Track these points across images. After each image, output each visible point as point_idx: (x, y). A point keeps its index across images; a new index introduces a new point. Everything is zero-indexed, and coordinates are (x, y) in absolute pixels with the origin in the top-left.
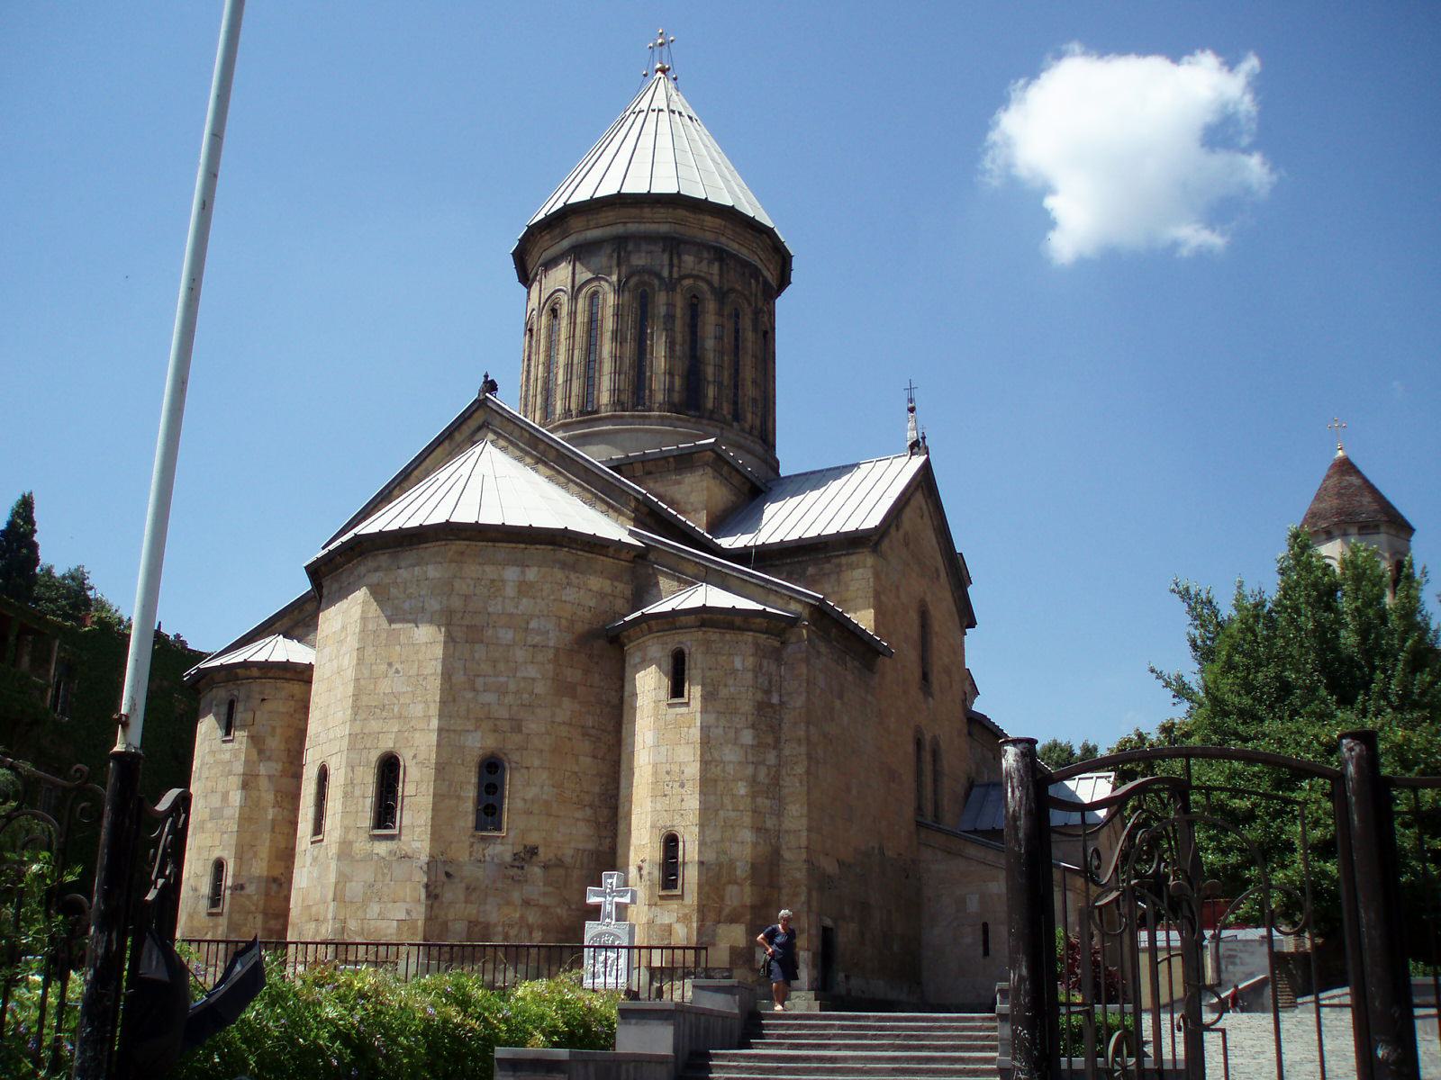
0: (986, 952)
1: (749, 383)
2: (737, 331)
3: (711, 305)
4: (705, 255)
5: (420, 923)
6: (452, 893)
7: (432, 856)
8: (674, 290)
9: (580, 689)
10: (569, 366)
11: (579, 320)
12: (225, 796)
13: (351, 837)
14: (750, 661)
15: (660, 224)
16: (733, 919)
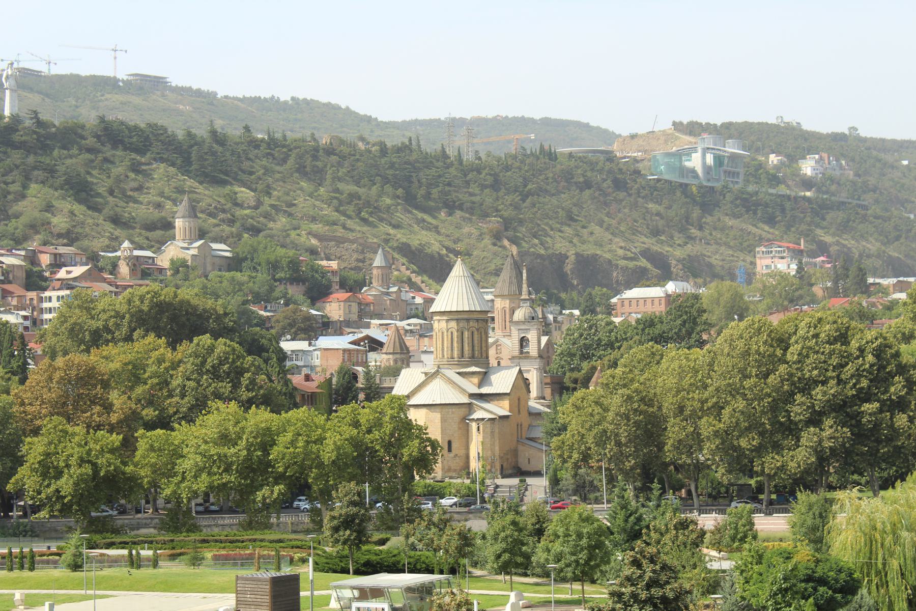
3: (476, 333)
6: (445, 462)
10: (447, 347)
15: (465, 316)
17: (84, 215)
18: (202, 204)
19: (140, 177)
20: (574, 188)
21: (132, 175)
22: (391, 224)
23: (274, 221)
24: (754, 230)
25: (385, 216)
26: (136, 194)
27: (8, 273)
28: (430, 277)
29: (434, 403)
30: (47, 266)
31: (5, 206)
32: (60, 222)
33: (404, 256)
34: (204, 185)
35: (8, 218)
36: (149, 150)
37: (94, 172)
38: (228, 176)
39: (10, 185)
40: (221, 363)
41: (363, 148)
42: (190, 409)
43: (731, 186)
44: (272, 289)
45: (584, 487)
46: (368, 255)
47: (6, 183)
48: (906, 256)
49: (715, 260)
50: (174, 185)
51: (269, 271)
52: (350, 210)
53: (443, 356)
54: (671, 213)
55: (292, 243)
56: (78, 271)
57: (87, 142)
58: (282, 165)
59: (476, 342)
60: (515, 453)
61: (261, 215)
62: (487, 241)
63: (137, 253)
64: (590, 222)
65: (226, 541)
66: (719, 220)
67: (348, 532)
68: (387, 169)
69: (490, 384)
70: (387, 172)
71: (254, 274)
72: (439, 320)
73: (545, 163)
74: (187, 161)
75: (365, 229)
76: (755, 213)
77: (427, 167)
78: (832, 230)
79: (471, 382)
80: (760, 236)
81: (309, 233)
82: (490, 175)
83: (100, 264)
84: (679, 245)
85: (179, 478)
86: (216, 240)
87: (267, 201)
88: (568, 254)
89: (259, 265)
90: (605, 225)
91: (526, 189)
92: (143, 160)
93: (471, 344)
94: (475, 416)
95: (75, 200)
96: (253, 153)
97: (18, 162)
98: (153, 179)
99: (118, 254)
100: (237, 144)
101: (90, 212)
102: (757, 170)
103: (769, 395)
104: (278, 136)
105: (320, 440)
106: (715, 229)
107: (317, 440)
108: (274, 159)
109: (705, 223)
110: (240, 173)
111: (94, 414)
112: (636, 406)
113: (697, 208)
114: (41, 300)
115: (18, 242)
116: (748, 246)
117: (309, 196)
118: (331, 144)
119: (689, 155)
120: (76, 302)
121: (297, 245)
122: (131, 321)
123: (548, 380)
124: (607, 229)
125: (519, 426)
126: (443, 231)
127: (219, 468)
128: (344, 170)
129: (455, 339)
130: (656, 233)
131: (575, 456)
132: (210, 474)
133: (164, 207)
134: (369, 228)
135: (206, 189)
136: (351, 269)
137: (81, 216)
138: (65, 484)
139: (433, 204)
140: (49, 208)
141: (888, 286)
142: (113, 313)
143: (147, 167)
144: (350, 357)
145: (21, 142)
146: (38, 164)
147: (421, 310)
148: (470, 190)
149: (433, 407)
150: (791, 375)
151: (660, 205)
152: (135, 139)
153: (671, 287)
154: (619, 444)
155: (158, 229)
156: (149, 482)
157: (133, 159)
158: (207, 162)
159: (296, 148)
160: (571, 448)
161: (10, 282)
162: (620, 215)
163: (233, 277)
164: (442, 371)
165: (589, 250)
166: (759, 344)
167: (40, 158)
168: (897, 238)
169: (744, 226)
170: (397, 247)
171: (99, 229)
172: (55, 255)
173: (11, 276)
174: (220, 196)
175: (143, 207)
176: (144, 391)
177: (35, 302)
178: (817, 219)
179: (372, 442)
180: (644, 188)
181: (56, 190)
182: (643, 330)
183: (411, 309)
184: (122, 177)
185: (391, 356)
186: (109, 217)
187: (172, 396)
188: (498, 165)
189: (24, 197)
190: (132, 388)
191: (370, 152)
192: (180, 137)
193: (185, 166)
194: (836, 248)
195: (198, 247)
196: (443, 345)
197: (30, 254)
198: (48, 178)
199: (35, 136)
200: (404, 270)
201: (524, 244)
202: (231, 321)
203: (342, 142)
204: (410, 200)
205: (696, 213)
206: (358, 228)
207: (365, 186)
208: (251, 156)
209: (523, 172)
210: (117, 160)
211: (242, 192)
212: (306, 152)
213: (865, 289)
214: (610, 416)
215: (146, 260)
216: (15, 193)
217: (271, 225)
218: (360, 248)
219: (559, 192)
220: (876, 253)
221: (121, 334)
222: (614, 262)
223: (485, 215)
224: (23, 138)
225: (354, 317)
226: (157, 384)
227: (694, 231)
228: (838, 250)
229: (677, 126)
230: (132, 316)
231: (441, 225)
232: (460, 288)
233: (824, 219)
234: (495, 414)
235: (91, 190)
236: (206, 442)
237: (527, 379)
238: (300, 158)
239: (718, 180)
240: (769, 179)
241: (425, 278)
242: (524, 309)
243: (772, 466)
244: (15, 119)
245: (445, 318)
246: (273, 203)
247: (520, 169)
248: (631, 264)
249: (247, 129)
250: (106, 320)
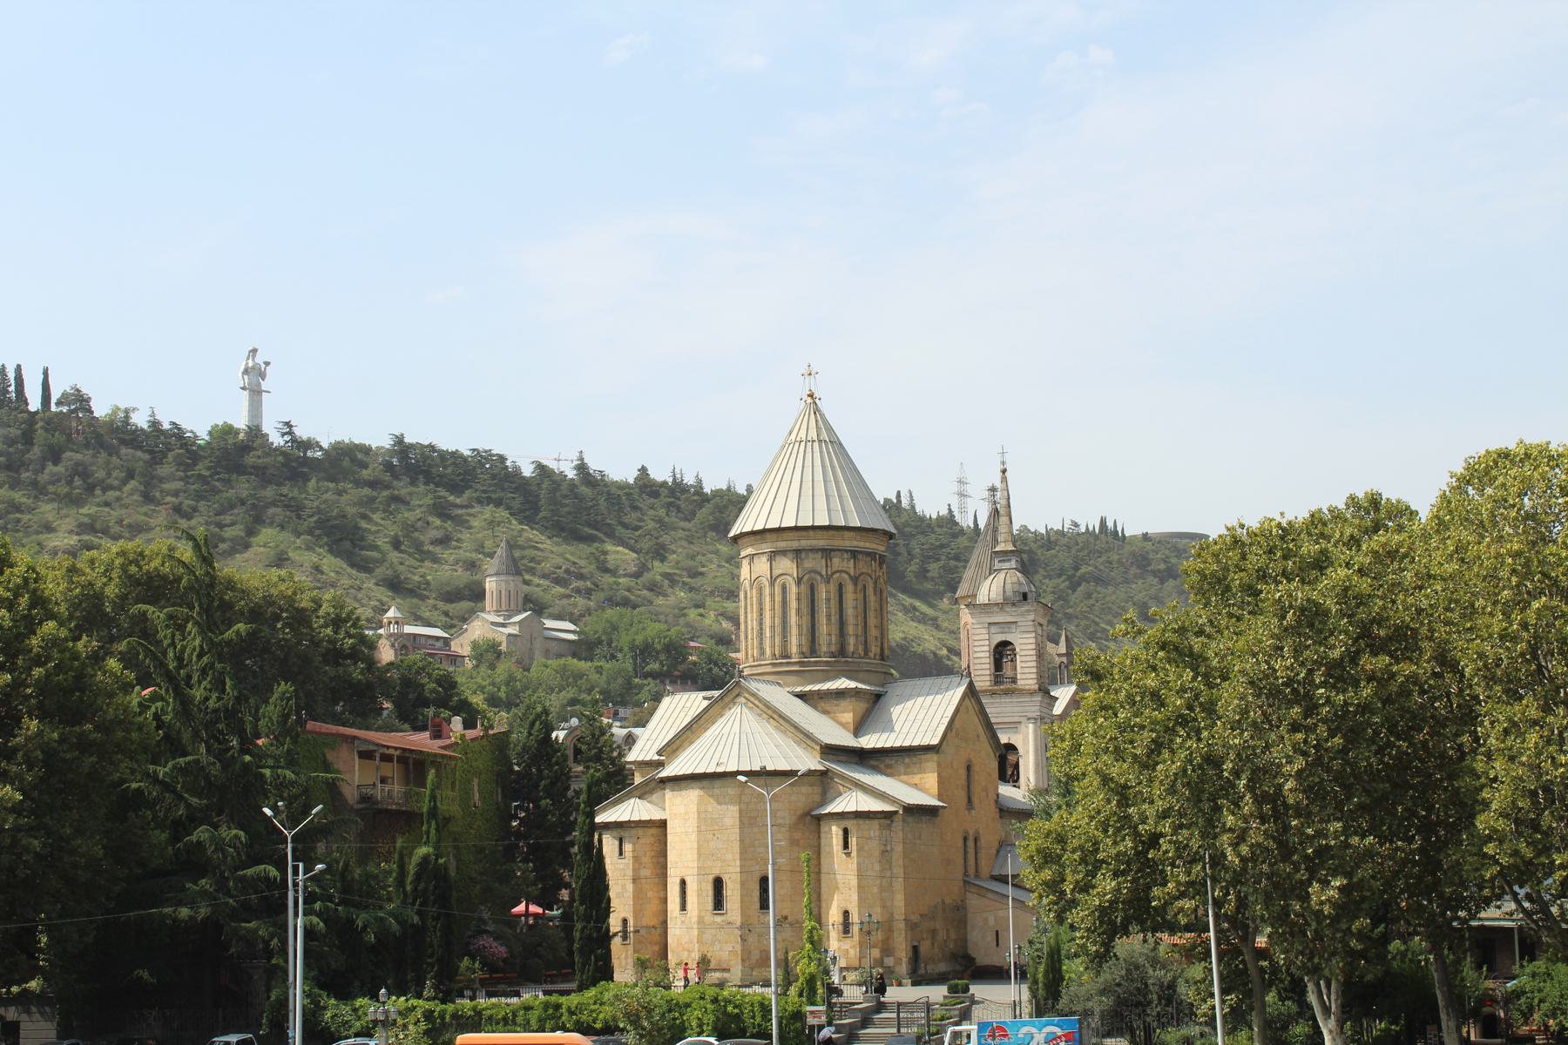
0: (998, 945)
1: (873, 629)
2: (865, 596)
3: (849, 588)
4: (846, 556)
5: (739, 952)
6: (751, 939)
7: (742, 924)
8: (828, 582)
9: (801, 842)
10: (773, 627)
11: (776, 599)
12: (624, 886)
13: (703, 914)
14: (877, 833)
15: (820, 542)
16: (875, 947)
17: (337, 572)
21: (438, 522)
23: (665, 595)
26: (438, 549)
29: (720, 769)
34: (555, 539)
36: (471, 487)
37: (376, 517)
38: (597, 530)
39: (226, 529)
45: (1143, 1005)
51: (635, 660)
58: (689, 521)
59: (850, 612)
60: (958, 915)
72: (752, 557)
73: (1107, 542)
74: (536, 509)
77: (923, 533)
89: (621, 650)
91: (1078, 574)
92: (458, 501)
93: (835, 618)
94: (836, 806)
95: (331, 551)
96: (645, 502)
97: (244, 494)
98: (470, 528)
101: (349, 570)
108: (679, 511)
110: (619, 527)
117: (727, 562)
125: (971, 842)
126: (945, 625)
129: (793, 604)
131: (1106, 884)
135: (558, 544)
137: (332, 574)
143: (464, 511)
146: (278, 497)
149: (718, 783)
157: (440, 497)
158: (567, 509)
160: (1091, 861)
163: (565, 665)
175: (447, 567)
186: (383, 580)
189: (247, 546)
195: (520, 623)
196: (761, 624)
202: (350, 636)
209: (1073, 552)
211: (618, 552)
215: (430, 642)
216: (232, 540)
217: (660, 601)
219: (1127, 581)
231: (942, 617)
232: (808, 470)
237: (1011, 748)
238: (721, 512)
242: (1002, 575)
245: (766, 547)
246: (668, 571)
247: (1069, 548)
249: (643, 470)
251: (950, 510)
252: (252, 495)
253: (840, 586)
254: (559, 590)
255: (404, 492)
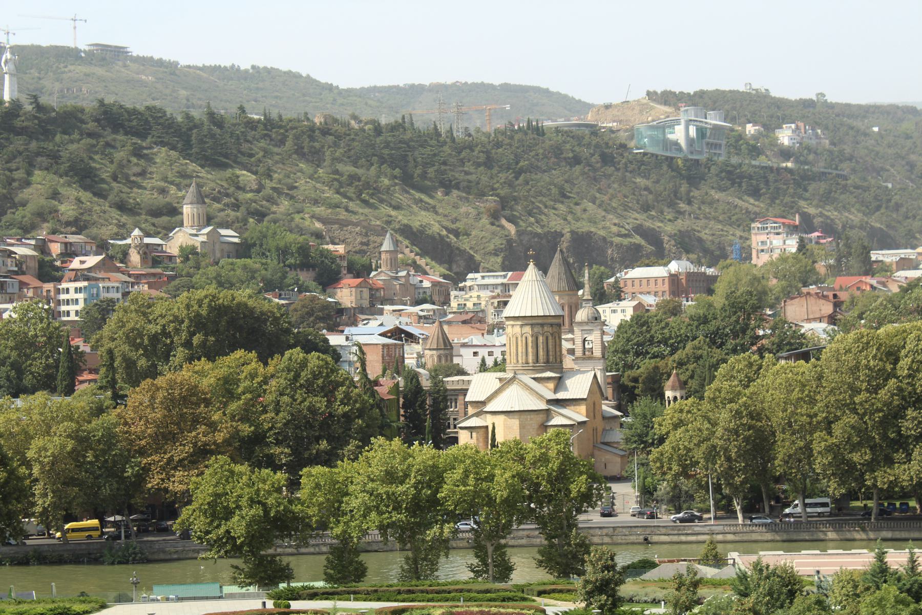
3: (550, 338)
15: (540, 321)
17: (91, 202)
18: (206, 189)
19: (142, 162)
20: (564, 164)
22: (391, 206)
23: (277, 204)
24: (740, 203)
25: (384, 197)
26: (139, 179)
27: (21, 264)
28: (432, 260)
30: (57, 255)
31: (10, 194)
32: (67, 210)
33: (406, 238)
35: (15, 206)
37: (96, 157)
38: (227, 158)
40: (316, 376)
41: (356, 126)
42: (285, 424)
43: (715, 158)
44: (284, 277)
45: (679, 497)
46: (372, 238)
47: (10, 170)
48: (887, 226)
49: (705, 235)
50: (176, 169)
51: (278, 256)
52: (351, 191)
53: (518, 361)
54: (659, 187)
55: (297, 226)
56: (92, 260)
57: (89, 126)
59: (550, 347)
61: (264, 199)
62: (485, 221)
63: (147, 240)
64: (582, 199)
65: (432, 592)
66: (707, 194)
67: (604, 597)
68: (384, 148)
69: (566, 389)
70: (383, 151)
71: (264, 261)
72: (513, 326)
73: (534, 139)
74: (188, 144)
75: (367, 211)
76: (740, 186)
77: (421, 146)
78: (815, 203)
79: (546, 387)
80: (747, 209)
81: (312, 217)
82: (483, 152)
83: (110, 252)
84: (670, 220)
85: (348, 517)
86: (227, 226)
87: (268, 184)
88: (564, 232)
90: (597, 202)
91: (518, 166)
92: (144, 144)
94: (553, 422)
95: (81, 186)
97: (21, 148)
98: (155, 163)
99: (129, 241)
100: (234, 125)
101: (96, 199)
102: (737, 141)
103: (879, 410)
104: (274, 115)
105: (491, 478)
106: (703, 203)
107: (486, 477)
108: (271, 140)
109: (693, 197)
111: (199, 434)
112: (745, 421)
113: (684, 181)
114: (58, 291)
115: (26, 230)
116: (737, 220)
118: (326, 123)
119: (672, 127)
120: (133, 307)
121: (301, 229)
122: (190, 326)
123: (610, 380)
124: (600, 206)
125: (595, 430)
126: (441, 211)
127: (388, 506)
128: (341, 150)
129: (530, 344)
130: (646, 208)
132: (381, 513)
133: (168, 192)
134: (370, 210)
135: (208, 172)
136: (356, 252)
138: (237, 526)
139: (429, 183)
140: (55, 195)
141: (891, 264)
142: (171, 318)
144: (388, 351)
145: (23, 128)
147: (428, 294)
148: (466, 169)
150: (900, 390)
151: (648, 179)
152: (134, 123)
153: (674, 266)
154: (728, 459)
155: (164, 215)
156: (317, 521)
157: (135, 144)
159: (292, 128)
161: (23, 273)
162: (611, 191)
164: (519, 376)
165: (584, 227)
166: (870, 359)
167: (42, 144)
168: (878, 208)
169: (731, 199)
170: (399, 229)
171: (107, 216)
172: (66, 244)
173: (24, 267)
174: (221, 180)
176: (239, 406)
177: (52, 294)
178: (800, 191)
179: (538, 478)
180: (631, 162)
181: (61, 176)
182: (697, 327)
183: (419, 293)
184: (125, 162)
185: (434, 352)
187: (267, 412)
188: (490, 142)
189: (28, 184)
190: (225, 405)
191: (364, 131)
192: (180, 119)
193: (186, 152)
194: (820, 219)
195: (207, 234)
197: (40, 243)
198: (52, 164)
199: (36, 121)
200: (408, 253)
201: (521, 223)
203: (336, 121)
204: (408, 181)
205: (684, 188)
206: (361, 211)
207: (362, 166)
208: (249, 138)
209: (514, 148)
210: (118, 145)
211: (244, 175)
212: (303, 132)
213: (869, 268)
214: (720, 432)
216: (20, 180)
217: (274, 208)
218: (364, 231)
219: (550, 169)
220: (858, 225)
221: (180, 339)
222: (609, 239)
223: (481, 195)
224: (25, 124)
225: (366, 303)
226: (251, 399)
227: (683, 206)
228: (822, 222)
229: (651, 95)
230: (191, 320)
231: (438, 205)
233: (806, 190)
234: (574, 420)
235: (96, 176)
236: (373, 480)
239: (700, 153)
240: (749, 150)
241: (429, 260)
242: (586, 310)
243: (886, 480)
244: (16, 105)
245: (520, 323)
246: (274, 185)
247: (511, 145)
248: (626, 241)
249: (242, 109)
250: (164, 326)
251: (436, 126)
252: (26, 149)
253: (547, 338)
254: (217, 205)
255: (109, 139)
